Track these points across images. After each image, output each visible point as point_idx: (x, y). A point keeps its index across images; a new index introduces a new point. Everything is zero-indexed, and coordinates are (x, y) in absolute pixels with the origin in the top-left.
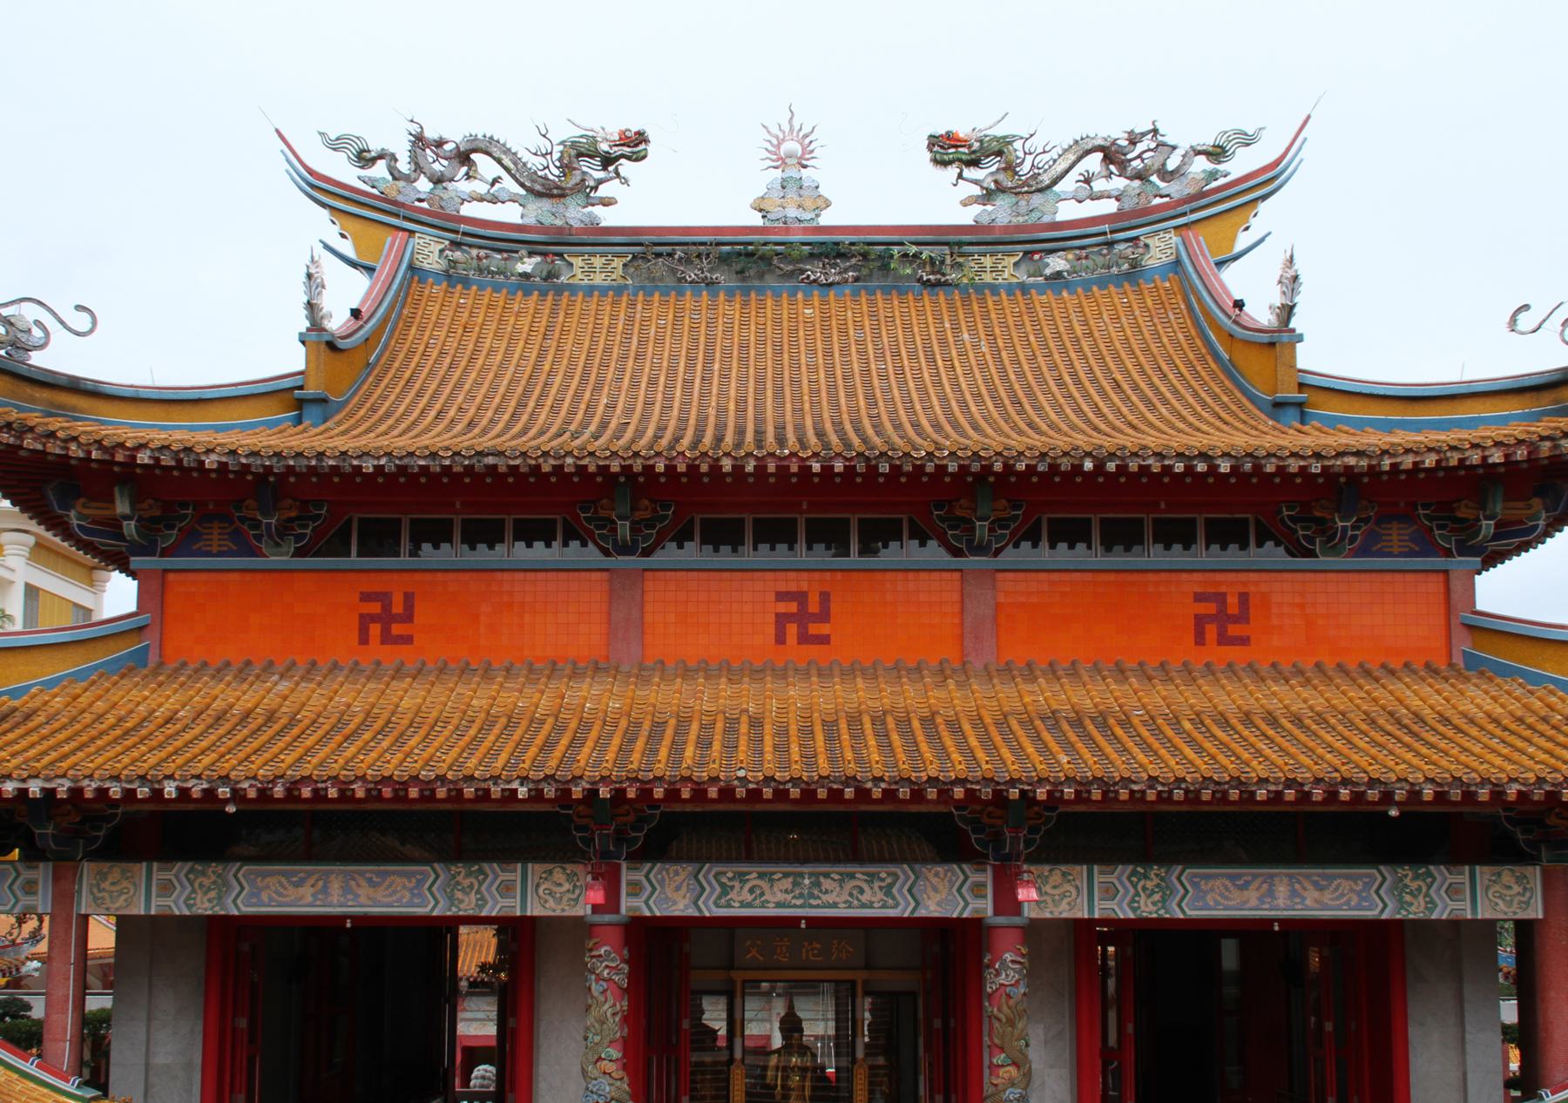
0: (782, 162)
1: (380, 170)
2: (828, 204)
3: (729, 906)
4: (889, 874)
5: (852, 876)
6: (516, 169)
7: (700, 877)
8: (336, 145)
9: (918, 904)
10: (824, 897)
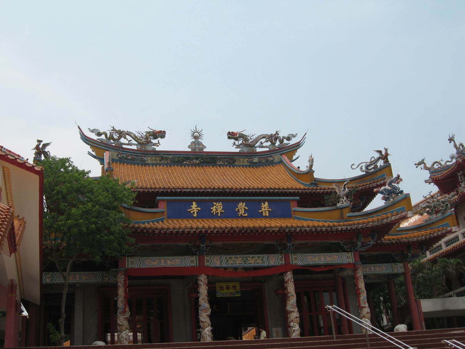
0: (196, 138)
1: (103, 137)
3: (228, 264)
4: (262, 256)
5: (254, 257)
6: (135, 138)
7: (222, 258)
9: (269, 263)
10: (249, 262)
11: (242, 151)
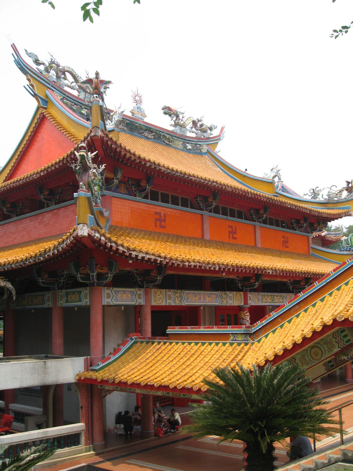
0: (136, 101)
2: (146, 117)
8: (30, 55)
11: (175, 131)
